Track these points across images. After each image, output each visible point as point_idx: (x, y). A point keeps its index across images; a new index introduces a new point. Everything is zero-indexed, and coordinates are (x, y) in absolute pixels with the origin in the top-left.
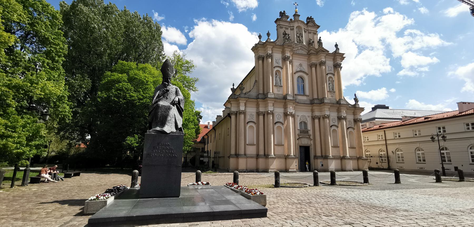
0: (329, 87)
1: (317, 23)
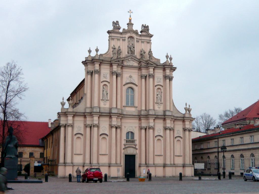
0: (157, 98)
1: (151, 32)
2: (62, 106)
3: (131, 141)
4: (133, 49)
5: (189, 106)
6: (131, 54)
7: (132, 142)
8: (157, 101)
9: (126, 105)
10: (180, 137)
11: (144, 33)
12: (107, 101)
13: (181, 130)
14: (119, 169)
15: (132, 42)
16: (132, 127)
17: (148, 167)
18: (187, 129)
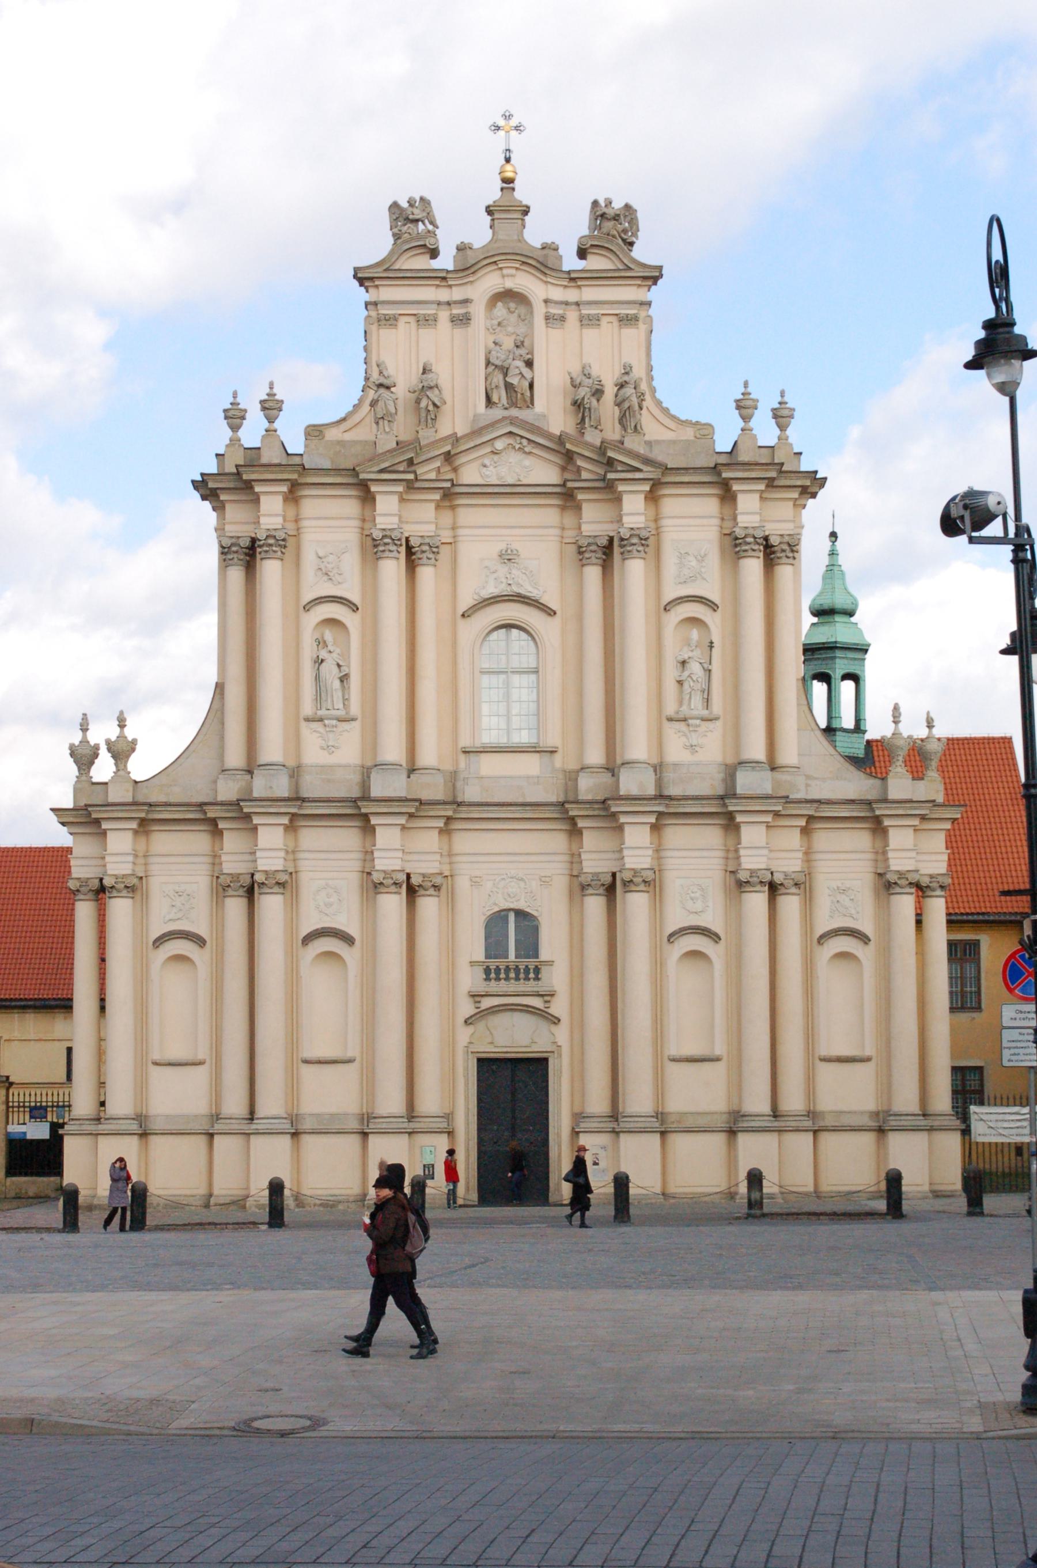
0: (680, 683)
2: (79, 769)
6: (506, 409)
7: (522, 976)
8: (681, 703)
11: (596, 262)
12: (346, 726)
16: (522, 880)
18: (901, 882)
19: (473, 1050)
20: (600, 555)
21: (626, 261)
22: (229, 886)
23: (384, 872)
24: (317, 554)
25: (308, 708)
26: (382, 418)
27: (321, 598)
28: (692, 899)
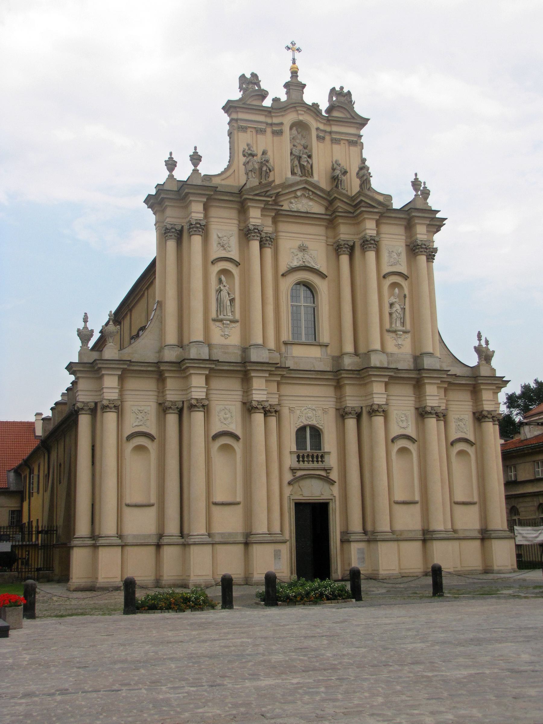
0: (391, 314)
1: (360, 109)
2: (82, 342)
3: (313, 457)
4: (307, 161)
5: (487, 342)
6: (301, 177)
7: (315, 459)
8: (391, 323)
9: (293, 338)
10: (466, 441)
12: (233, 325)
13: (468, 418)
14: (280, 551)
15: (303, 142)
16: (314, 410)
17: (376, 541)
18: (489, 416)
19: (293, 498)
20: (349, 250)
21: (353, 115)
22: (170, 408)
23: (258, 401)
24: (218, 235)
25: (213, 315)
26: (251, 171)
27: (221, 258)
28: (402, 421)
